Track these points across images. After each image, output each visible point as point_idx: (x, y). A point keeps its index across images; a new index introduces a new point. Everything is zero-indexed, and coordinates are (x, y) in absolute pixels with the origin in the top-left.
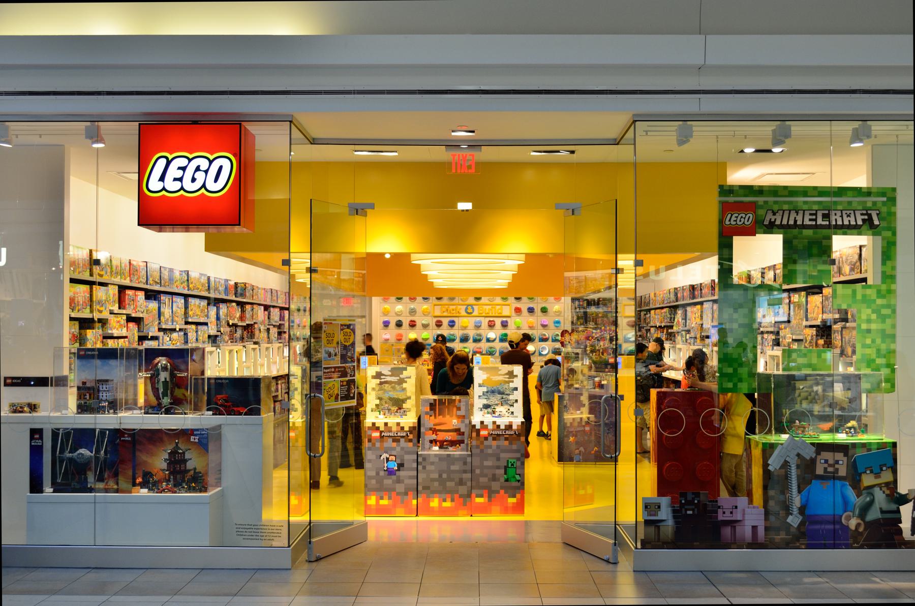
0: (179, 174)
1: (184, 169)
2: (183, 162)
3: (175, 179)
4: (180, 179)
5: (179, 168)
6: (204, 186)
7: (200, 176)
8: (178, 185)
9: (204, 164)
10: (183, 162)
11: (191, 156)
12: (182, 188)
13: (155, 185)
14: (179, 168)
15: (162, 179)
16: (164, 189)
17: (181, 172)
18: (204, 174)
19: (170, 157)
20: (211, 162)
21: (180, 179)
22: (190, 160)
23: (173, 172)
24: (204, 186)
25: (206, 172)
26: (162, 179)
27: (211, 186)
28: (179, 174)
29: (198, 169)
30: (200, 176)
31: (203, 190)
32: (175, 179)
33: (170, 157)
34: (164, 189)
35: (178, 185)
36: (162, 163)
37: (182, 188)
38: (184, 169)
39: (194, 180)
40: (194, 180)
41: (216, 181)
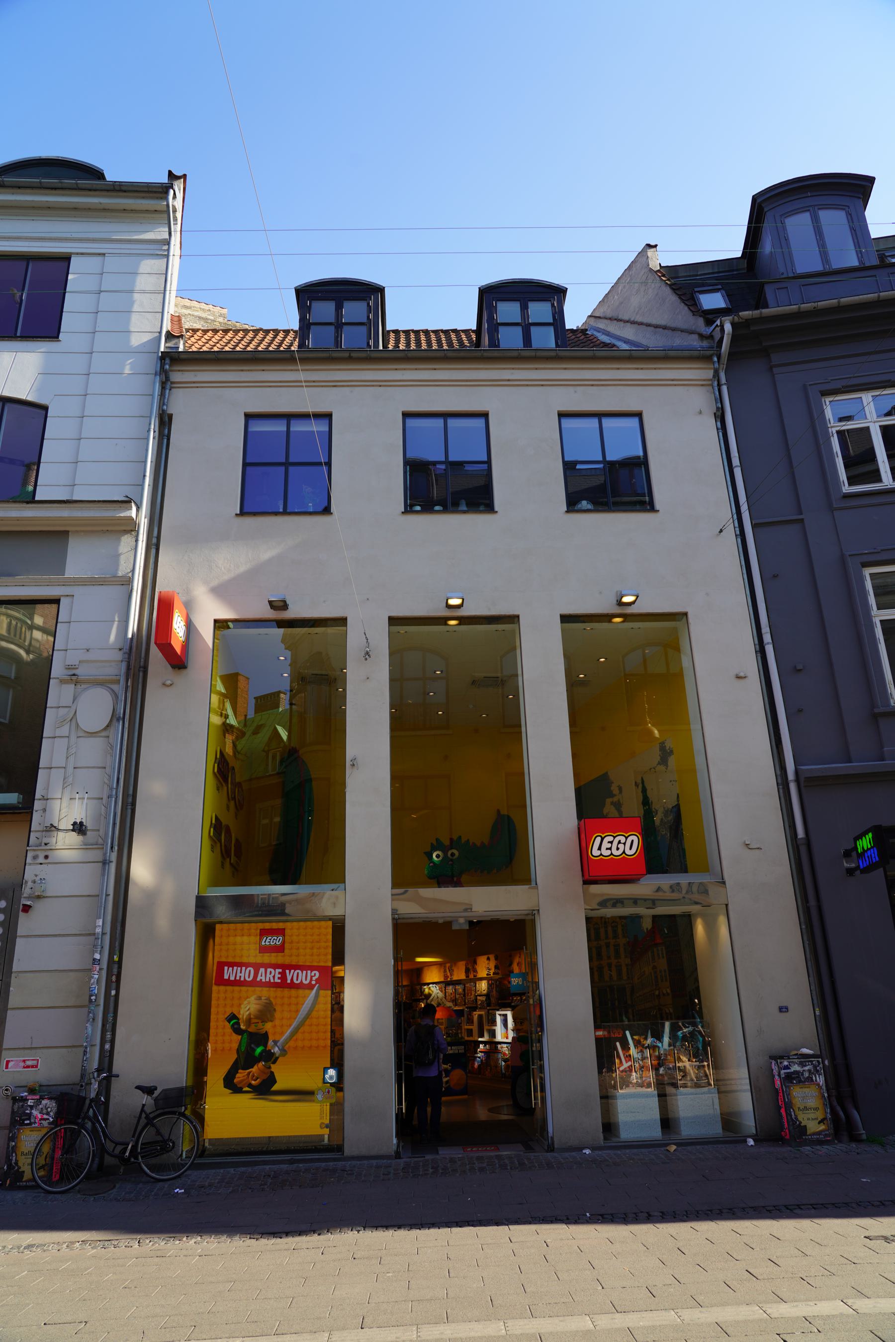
0: (609, 845)
1: (611, 842)
2: (611, 839)
4: (610, 849)
6: (624, 852)
7: (621, 846)
8: (609, 852)
9: (623, 839)
10: (611, 839)
12: (612, 854)
13: (596, 852)
15: (599, 849)
16: (601, 855)
20: (626, 838)
21: (610, 849)
22: (615, 837)
23: (605, 844)
24: (624, 852)
25: (624, 844)
26: (599, 849)
27: (628, 852)
28: (609, 845)
29: (619, 842)
30: (621, 846)
34: (601, 855)
35: (609, 852)
36: (598, 839)
37: (612, 854)
38: (611, 842)
39: (618, 849)
40: (618, 849)
41: (631, 849)
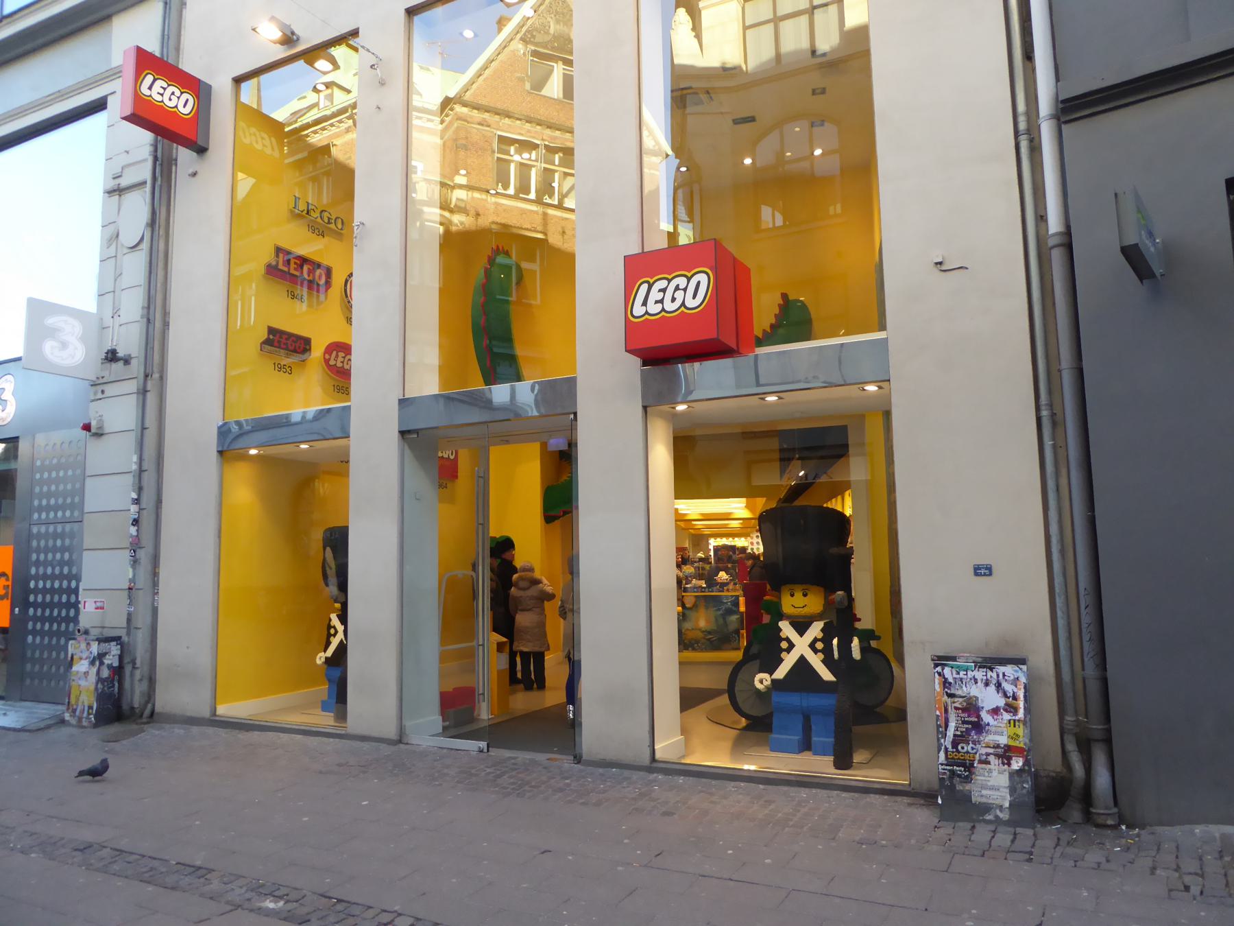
1: (664, 290)
3: (657, 302)
4: (661, 301)
5: (660, 291)
6: (683, 304)
8: (659, 307)
10: (663, 284)
12: (663, 310)
13: (638, 310)
14: (660, 291)
15: (645, 303)
16: (647, 313)
20: (689, 279)
21: (661, 301)
22: (669, 281)
23: (655, 295)
24: (683, 304)
25: (685, 290)
26: (645, 303)
29: (677, 288)
32: (657, 302)
34: (647, 313)
35: (659, 307)
36: (645, 287)
37: (663, 310)
38: (664, 290)
39: (673, 300)
40: (673, 300)
41: (694, 297)
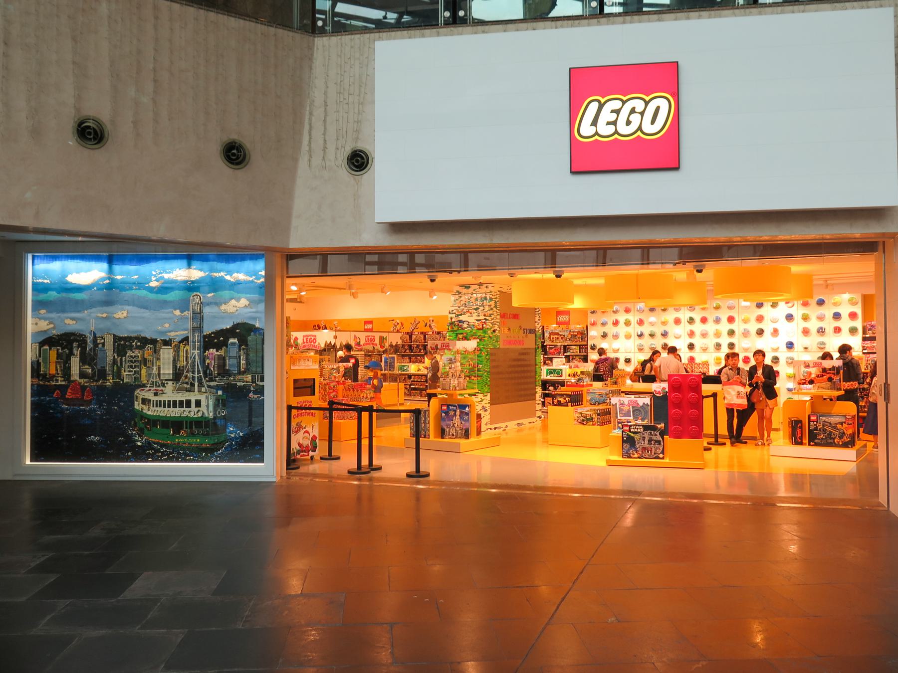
0: (613, 117)
1: (618, 112)
2: (617, 105)
3: (608, 123)
4: (614, 123)
5: (612, 111)
6: (640, 128)
8: (611, 129)
9: (639, 105)
10: (617, 105)
11: (625, 98)
12: (616, 132)
13: (587, 129)
14: (612, 111)
15: (594, 123)
16: (597, 133)
17: (615, 115)
18: (639, 116)
19: (603, 100)
20: (647, 103)
21: (614, 123)
22: (624, 102)
23: (607, 115)
24: (640, 128)
25: (642, 114)
26: (594, 123)
27: (648, 128)
28: (613, 117)
29: (633, 111)
31: (639, 133)
32: (608, 123)
33: (603, 100)
34: (597, 133)
35: (611, 129)
36: (594, 106)
37: (616, 132)
38: (618, 112)
39: (628, 123)
40: (628, 123)
41: (653, 122)
